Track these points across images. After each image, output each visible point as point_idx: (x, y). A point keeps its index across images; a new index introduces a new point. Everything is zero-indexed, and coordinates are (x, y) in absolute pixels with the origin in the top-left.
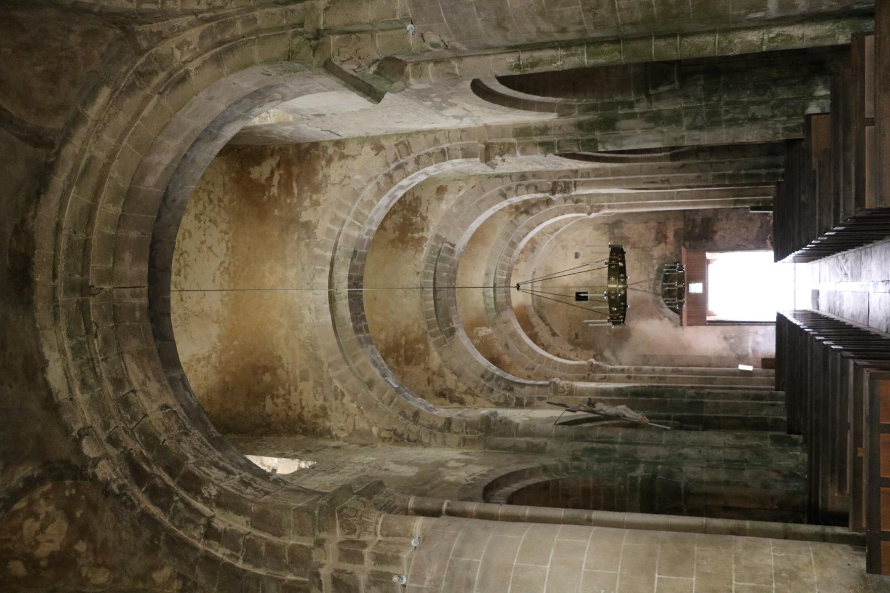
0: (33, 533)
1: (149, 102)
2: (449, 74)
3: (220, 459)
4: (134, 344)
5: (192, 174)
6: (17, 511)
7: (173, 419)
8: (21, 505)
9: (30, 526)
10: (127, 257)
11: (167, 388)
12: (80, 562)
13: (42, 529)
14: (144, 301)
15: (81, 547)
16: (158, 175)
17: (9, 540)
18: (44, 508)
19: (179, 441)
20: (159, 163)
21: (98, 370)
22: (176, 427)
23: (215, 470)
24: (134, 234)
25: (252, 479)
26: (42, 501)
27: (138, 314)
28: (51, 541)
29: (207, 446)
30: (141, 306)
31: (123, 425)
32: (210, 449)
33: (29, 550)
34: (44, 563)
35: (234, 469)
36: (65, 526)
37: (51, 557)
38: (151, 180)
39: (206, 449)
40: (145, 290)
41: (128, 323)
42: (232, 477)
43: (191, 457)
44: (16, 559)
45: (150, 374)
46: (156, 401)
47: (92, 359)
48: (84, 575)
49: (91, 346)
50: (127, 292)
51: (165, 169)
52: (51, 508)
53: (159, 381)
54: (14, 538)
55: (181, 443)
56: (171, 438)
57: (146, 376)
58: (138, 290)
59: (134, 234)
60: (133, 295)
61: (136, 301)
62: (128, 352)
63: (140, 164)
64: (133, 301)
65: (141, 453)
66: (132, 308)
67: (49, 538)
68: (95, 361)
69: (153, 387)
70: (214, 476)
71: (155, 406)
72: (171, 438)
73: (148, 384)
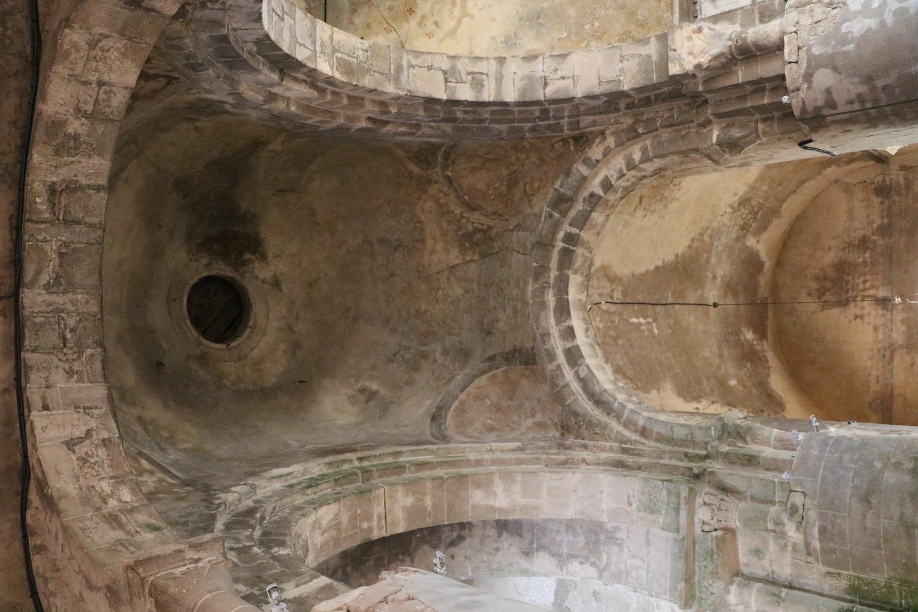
1: (534, 464)
2: (774, 594)
4: (345, 519)
5: (483, 561)
8: (145, 464)
10: (409, 501)
11: (317, 558)
14: (376, 535)
16: (483, 503)
20: (495, 494)
21: (309, 491)
24: (428, 501)
26: (155, 479)
27: (365, 525)
30: (370, 529)
38: (477, 497)
40: (384, 534)
41: (359, 511)
49: (326, 485)
50: (381, 509)
51: (491, 507)
58: (383, 522)
59: (428, 501)
60: (379, 517)
61: (375, 523)
62: (339, 509)
63: (491, 473)
64: (375, 516)
66: (369, 519)
68: (315, 489)
69: (318, 539)
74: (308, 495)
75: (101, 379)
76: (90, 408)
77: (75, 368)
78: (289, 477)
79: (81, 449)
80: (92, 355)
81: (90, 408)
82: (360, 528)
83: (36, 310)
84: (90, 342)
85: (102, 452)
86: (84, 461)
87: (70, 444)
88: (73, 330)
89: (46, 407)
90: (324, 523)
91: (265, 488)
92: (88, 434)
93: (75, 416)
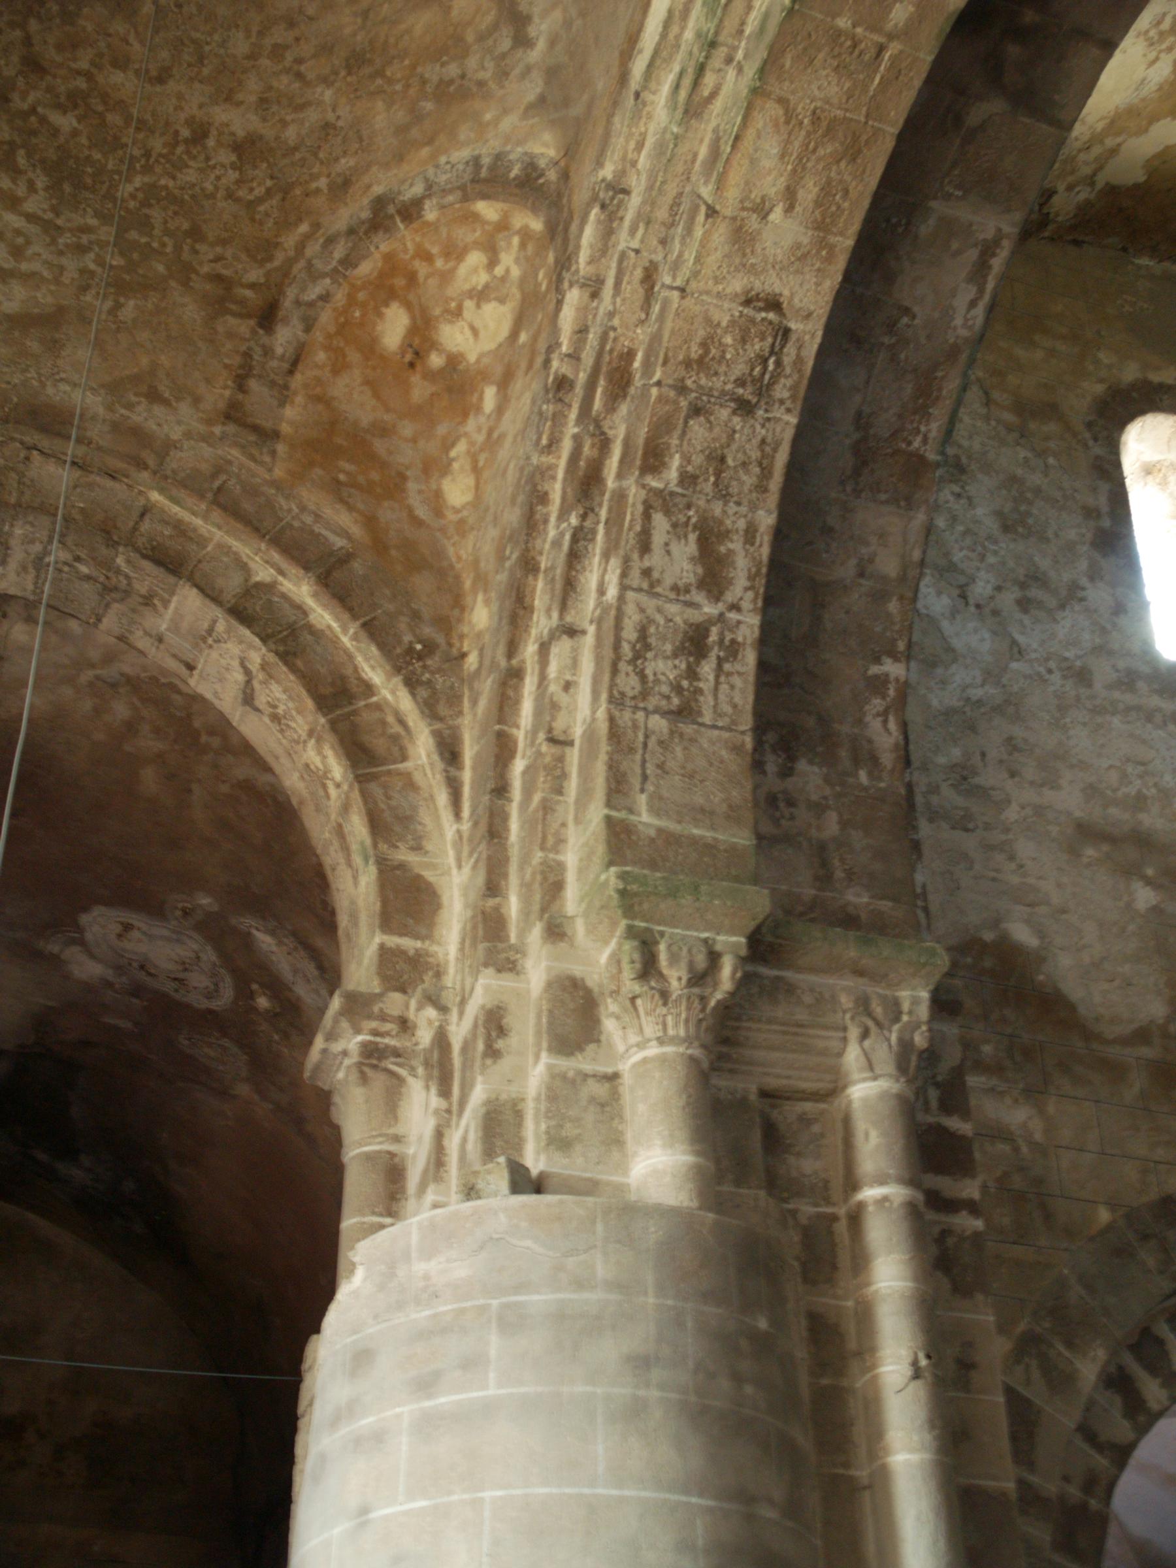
0: (467, 287)
3: (750, 534)
4: (821, 88)
6: (476, 217)
7: (757, 346)
8: (489, 210)
9: (472, 269)
12: (471, 425)
13: (481, 296)
15: (490, 397)
17: (429, 258)
18: (509, 262)
19: (696, 411)
21: (709, 80)
22: (739, 369)
23: (686, 550)
25: (733, 650)
26: (516, 240)
28: (475, 331)
29: (766, 473)
31: (658, 257)
32: (761, 488)
33: (437, 311)
34: (436, 361)
35: (741, 582)
36: (505, 331)
37: (454, 361)
39: (749, 480)
41: (843, 23)
42: (699, 597)
43: (672, 474)
44: (408, 306)
45: (808, 193)
46: (752, 270)
47: (713, 45)
48: (453, 454)
52: (516, 272)
53: (822, 226)
54: (439, 263)
55: (697, 428)
56: (682, 389)
57: (790, 196)
62: (781, 101)
65: (630, 355)
67: (478, 324)
68: (722, 52)
69: (783, 231)
70: (655, 559)
71: (737, 285)
72: (682, 389)
73: (776, 216)
74: (714, 95)
75: (172, 579)
76: (210, 631)
77: (143, 591)
78: (675, 30)
79: (261, 700)
80: (128, 562)
81: (210, 631)
82: (891, 37)
83: (30, 587)
84: (104, 551)
85: (277, 691)
86: (275, 718)
87: (248, 699)
88: (78, 559)
89: (191, 668)
90: (771, 185)
91: (640, 146)
92: (247, 672)
93: (214, 655)
